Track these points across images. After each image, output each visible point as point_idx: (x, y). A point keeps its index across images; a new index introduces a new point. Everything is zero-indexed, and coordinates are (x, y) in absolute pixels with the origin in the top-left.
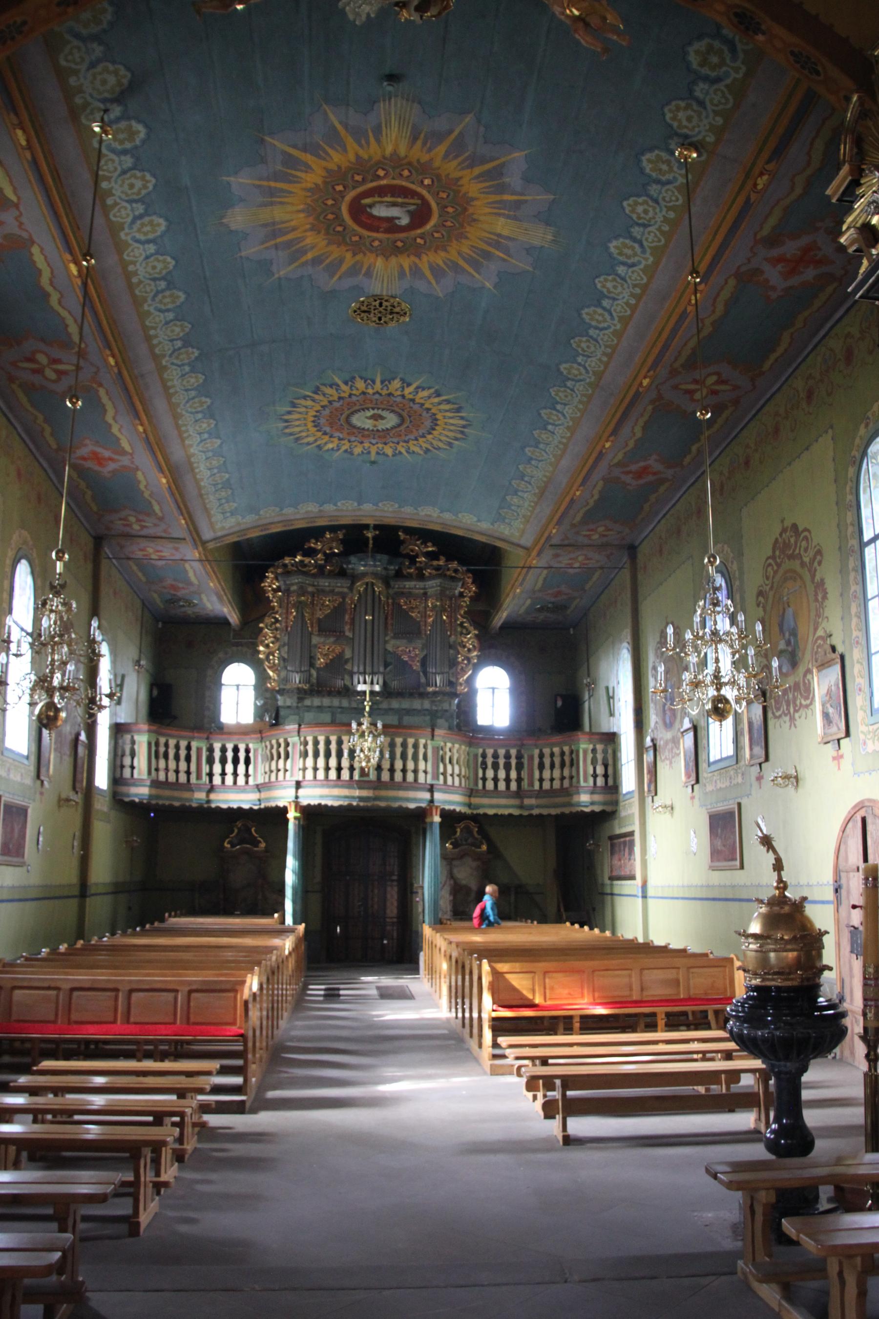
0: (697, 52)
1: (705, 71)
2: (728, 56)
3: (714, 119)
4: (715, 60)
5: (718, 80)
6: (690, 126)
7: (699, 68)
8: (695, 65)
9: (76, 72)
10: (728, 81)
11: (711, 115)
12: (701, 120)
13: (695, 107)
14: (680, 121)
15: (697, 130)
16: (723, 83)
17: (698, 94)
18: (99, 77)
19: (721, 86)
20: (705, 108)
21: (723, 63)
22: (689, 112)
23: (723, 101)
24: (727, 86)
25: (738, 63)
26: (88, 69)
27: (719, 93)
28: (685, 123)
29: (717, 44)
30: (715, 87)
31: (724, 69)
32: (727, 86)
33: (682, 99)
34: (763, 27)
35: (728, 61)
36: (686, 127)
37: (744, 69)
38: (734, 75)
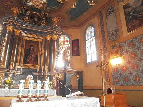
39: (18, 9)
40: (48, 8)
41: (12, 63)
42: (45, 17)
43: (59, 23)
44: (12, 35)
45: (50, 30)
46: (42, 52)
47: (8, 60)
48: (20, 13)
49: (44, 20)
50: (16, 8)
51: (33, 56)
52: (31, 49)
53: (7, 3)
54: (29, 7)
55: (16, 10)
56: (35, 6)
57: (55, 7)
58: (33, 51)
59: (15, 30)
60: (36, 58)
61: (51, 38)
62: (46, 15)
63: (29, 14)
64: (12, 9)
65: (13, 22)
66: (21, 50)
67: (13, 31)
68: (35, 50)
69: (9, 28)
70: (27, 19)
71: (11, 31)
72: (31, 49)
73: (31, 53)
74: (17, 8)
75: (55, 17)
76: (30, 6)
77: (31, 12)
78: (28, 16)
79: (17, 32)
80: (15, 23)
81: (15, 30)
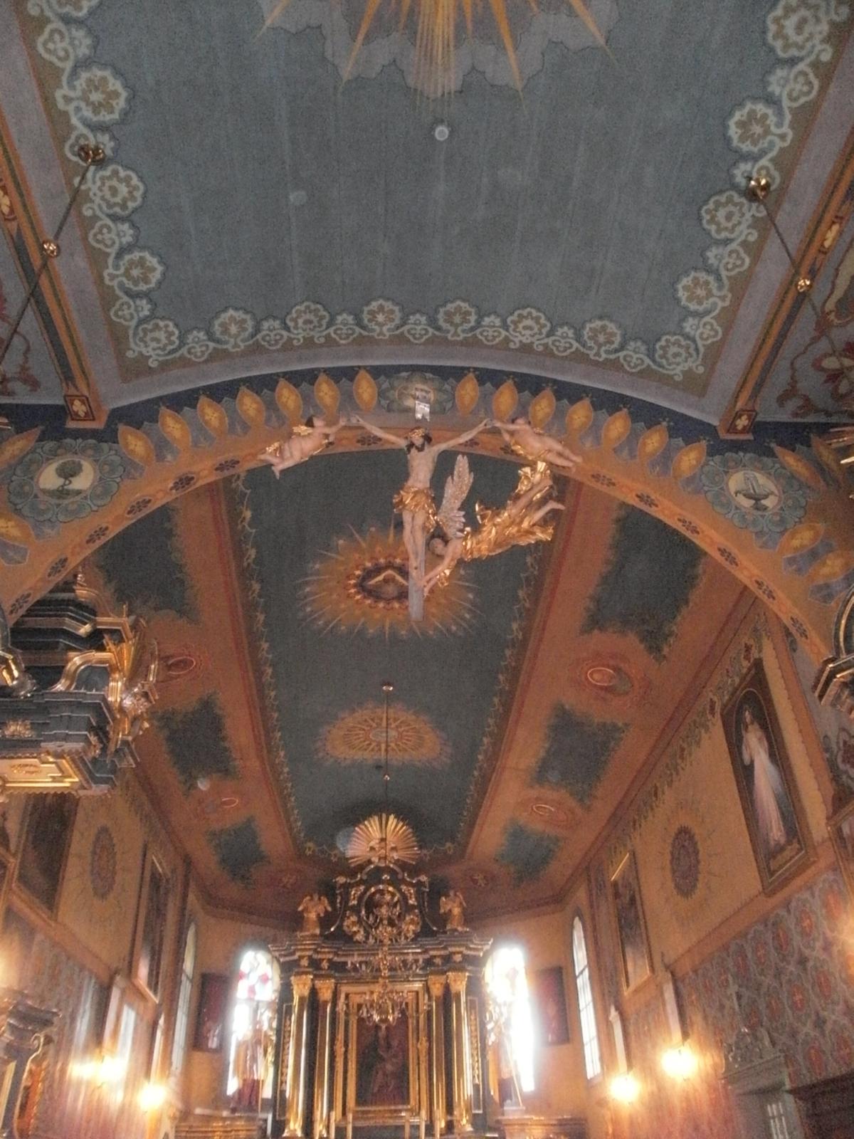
0: (154, 269)
1: (136, 255)
2: (129, 284)
3: (93, 209)
4: (135, 272)
5: (119, 255)
6: (108, 184)
7: (141, 254)
8: (147, 255)
9: (745, 244)
10: (110, 261)
11: (98, 213)
12: (103, 198)
13: (117, 210)
14: (120, 180)
15: (99, 183)
16: (113, 256)
17: (125, 227)
18: (730, 225)
19: (113, 251)
20: (109, 216)
21: (127, 274)
22: (118, 199)
23: (99, 237)
24: (108, 255)
25: (115, 283)
26: (732, 240)
27: (109, 243)
28: (114, 182)
29: (143, 287)
30: (117, 246)
31: (122, 270)
32: (108, 255)
33: (135, 211)
34: (174, 491)
35: (124, 280)
36: (109, 178)
37: (107, 281)
38: (111, 270)
39: (320, 899)
40: (425, 852)
41: (317, 1114)
42: (419, 895)
43: (468, 919)
44: (313, 1003)
45: (438, 949)
46: (417, 1047)
47: (307, 1108)
48: (326, 911)
49: (413, 907)
50: (312, 899)
51: (389, 1067)
52: (382, 1042)
53: (285, 880)
54: (352, 872)
55: (314, 909)
56: (375, 859)
57: (448, 844)
58: (389, 1046)
59: (318, 983)
60: (402, 1076)
61: (447, 988)
62: (420, 884)
63: (360, 899)
64: (300, 909)
65: (310, 957)
66: (346, 1052)
67: (314, 992)
68: (395, 1043)
69: (300, 989)
70: (354, 924)
71: (306, 993)
72: (382, 1042)
73: (382, 1059)
74: (316, 897)
75: (452, 893)
76: (361, 868)
77: (365, 892)
78: (356, 910)
79: (326, 995)
80: (315, 956)
81: (318, 983)
